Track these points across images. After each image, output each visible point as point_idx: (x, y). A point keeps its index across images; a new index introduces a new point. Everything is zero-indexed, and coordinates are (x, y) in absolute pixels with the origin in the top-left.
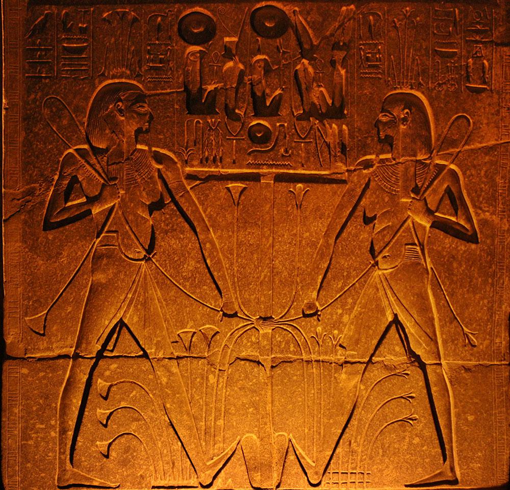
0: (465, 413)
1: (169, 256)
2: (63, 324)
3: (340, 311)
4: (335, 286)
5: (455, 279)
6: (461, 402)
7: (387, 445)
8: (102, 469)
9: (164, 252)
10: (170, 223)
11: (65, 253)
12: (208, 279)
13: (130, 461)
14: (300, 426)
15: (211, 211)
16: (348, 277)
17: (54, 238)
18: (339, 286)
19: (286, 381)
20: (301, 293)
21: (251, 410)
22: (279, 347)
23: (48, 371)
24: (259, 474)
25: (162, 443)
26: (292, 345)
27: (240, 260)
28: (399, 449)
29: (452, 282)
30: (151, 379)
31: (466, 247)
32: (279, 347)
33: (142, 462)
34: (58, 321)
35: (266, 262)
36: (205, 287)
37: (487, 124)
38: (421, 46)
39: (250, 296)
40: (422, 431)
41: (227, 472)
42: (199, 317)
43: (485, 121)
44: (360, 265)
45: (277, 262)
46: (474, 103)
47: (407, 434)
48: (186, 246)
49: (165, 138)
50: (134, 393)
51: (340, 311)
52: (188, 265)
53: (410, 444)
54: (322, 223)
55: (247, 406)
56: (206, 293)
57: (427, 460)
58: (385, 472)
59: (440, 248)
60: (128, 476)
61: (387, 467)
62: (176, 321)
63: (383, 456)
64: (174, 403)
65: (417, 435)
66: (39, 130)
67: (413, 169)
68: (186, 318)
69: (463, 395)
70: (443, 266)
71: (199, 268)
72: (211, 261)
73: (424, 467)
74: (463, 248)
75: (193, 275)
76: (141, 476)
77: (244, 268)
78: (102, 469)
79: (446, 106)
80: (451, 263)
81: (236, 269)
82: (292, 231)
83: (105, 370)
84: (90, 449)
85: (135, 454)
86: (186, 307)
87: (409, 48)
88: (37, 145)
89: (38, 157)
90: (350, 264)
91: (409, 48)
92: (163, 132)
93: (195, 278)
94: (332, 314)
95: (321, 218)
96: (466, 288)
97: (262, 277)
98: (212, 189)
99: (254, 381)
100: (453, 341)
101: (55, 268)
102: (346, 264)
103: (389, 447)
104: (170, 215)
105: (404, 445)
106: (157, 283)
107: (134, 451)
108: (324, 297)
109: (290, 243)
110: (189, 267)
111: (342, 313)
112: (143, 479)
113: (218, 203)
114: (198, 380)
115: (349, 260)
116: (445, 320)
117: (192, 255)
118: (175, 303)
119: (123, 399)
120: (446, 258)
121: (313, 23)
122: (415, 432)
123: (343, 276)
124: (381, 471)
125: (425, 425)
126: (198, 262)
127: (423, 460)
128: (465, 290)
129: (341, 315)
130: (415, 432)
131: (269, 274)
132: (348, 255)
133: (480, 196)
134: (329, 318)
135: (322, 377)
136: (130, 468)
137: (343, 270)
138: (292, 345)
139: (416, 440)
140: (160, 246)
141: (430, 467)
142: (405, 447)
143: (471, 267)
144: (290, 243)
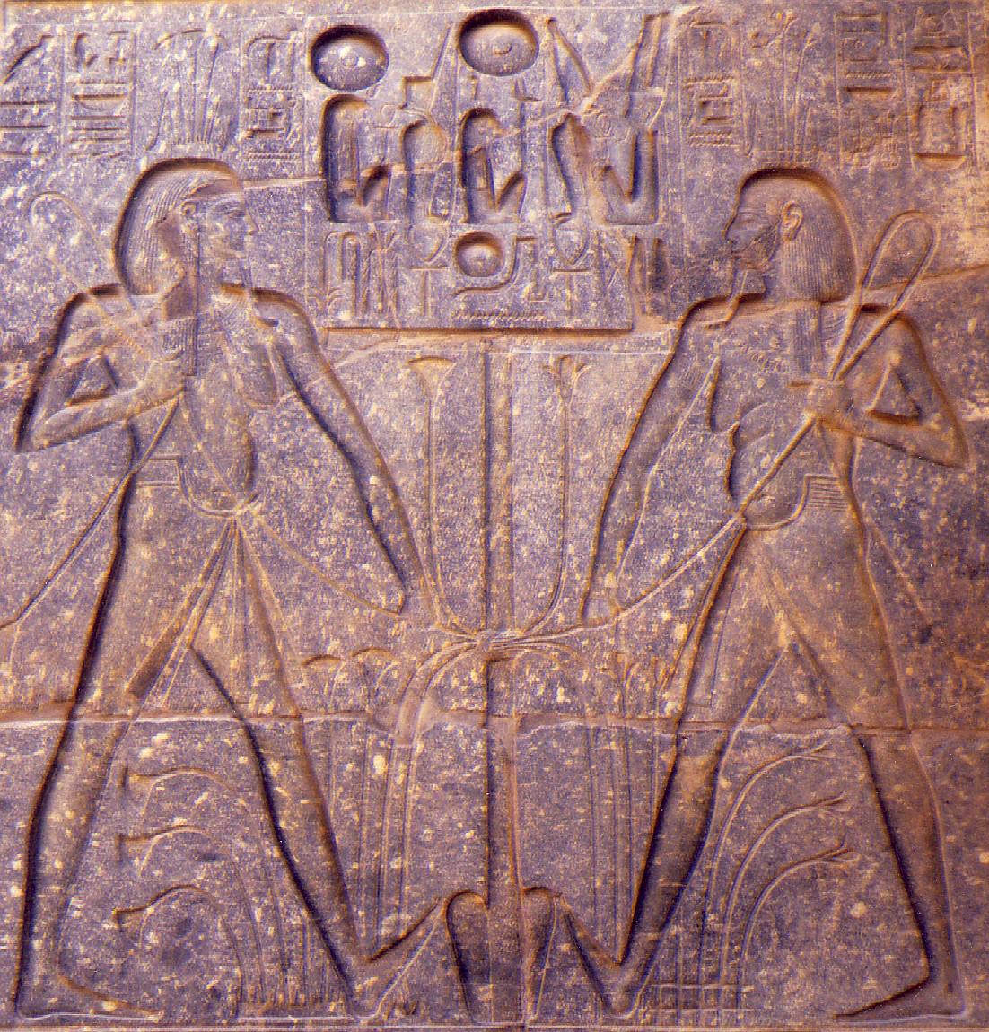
0: (972, 846)
1: (288, 502)
2: (52, 647)
3: (666, 616)
4: (653, 561)
5: (925, 545)
6: (959, 818)
7: (789, 921)
8: (123, 974)
9: (277, 494)
10: (290, 436)
11: (63, 499)
12: (373, 549)
13: (189, 954)
14: (583, 873)
15: (379, 410)
16: (681, 542)
17: (42, 469)
18: (663, 561)
19: (547, 769)
20: (578, 577)
21: (468, 835)
22: (532, 693)
23: (12, 749)
24: (491, 986)
25: (265, 910)
26: (560, 691)
27: (442, 510)
28: (818, 930)
29: (918, 550)
30: (244, 766)
31: (944, 476)
32: (532, 693)
33: (215, 956)
34: (42, 641)
35: (501, 514)
36: (366, 567)
37: (973, 229)
38: (817, 83)
39: (465, 584)
40: (871, 886)
41: (415, 981)
42: (352, 630)
43: (967, 224)
44: (707, 518)
45: (524, 513)
46: (940, 190)
47: (837, 893)
48: (325, 482)
49: (282, 268)
50: (204, 796)
51: (666, 616)
52: (330, 521)
53: (845, 918)
54: (619, 433)
55: (460, 825)
56: (369, 579)
57: (888, 958)
58: (790, 986)
59: (886, 482)
60: (182, 990)
61: (792, 973)
62: (302, 640)
63: (781, 945)
64: (295, 819)
65: (859, 898)
66: (20, 256)
67: (813, 321)
68: (323, 632)
69: (965, 804)
70: (895, 518)
71: (352, 527)
72: (381, 512)
73: (880, 976)
74: (939, 479)
75: (339, 541)
76: (214, 990)
77: (453, 527)
78: (123, 974)
79: (878, 195)
80: (914, 514)
81: (434, 528)
82: (555, 449)
83: (143, 746)
84: (99, 927)
85: (201, 938)
86: (324, 609)
87: (792, 90)
88: (13, 287)
89: (13, 310)
90: (685, 514)
91: (792, 90)
92: (277, 257)
93: (344, 548)
94: (648, 624)
95: (616, 423)
96: (952, 564)
97: (493, 544)
98: (380, 368)
99: (476, 769)
100: (931, 682)
101: (41, 531)
102: (677, 515)
103: (794, 924)
104: (291, 420)
105: (831, 921)
106: (262, 558)
107: (200, 932)
108: (631, 585)
109: (551, 475)
110: (331, 526)
111: (672, 620)
112: (218, 996)
113: (395, 394)
114: (349, 767)
115: (683, 508)
116: (908, 636)
117: (338, 500)
118: (299, 600)
119: (179, 812)
120: (902, 503)
121: (589, 46)
122: (854, 890)
123: (671, 541)
124: (778, 984)
125: (879, 872)
126: (351, 514)
127: (879, 956)
128: (952, 569)
129: (670, 625)
130: (854, 890)
131: (507, 538)
132: (679, 498)
133: (969, 373)
134: (642, 632)
135: (631, 759)
136: (188, 972)
137: (670, 528)
138: (560, 691)
139: (859, 910)
140: (269, 482)
141: (897, 975)
142: (833, 925)
143: (960, 520)
144: (551, 475)
